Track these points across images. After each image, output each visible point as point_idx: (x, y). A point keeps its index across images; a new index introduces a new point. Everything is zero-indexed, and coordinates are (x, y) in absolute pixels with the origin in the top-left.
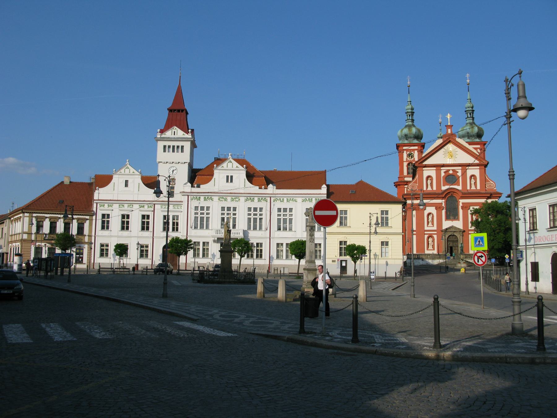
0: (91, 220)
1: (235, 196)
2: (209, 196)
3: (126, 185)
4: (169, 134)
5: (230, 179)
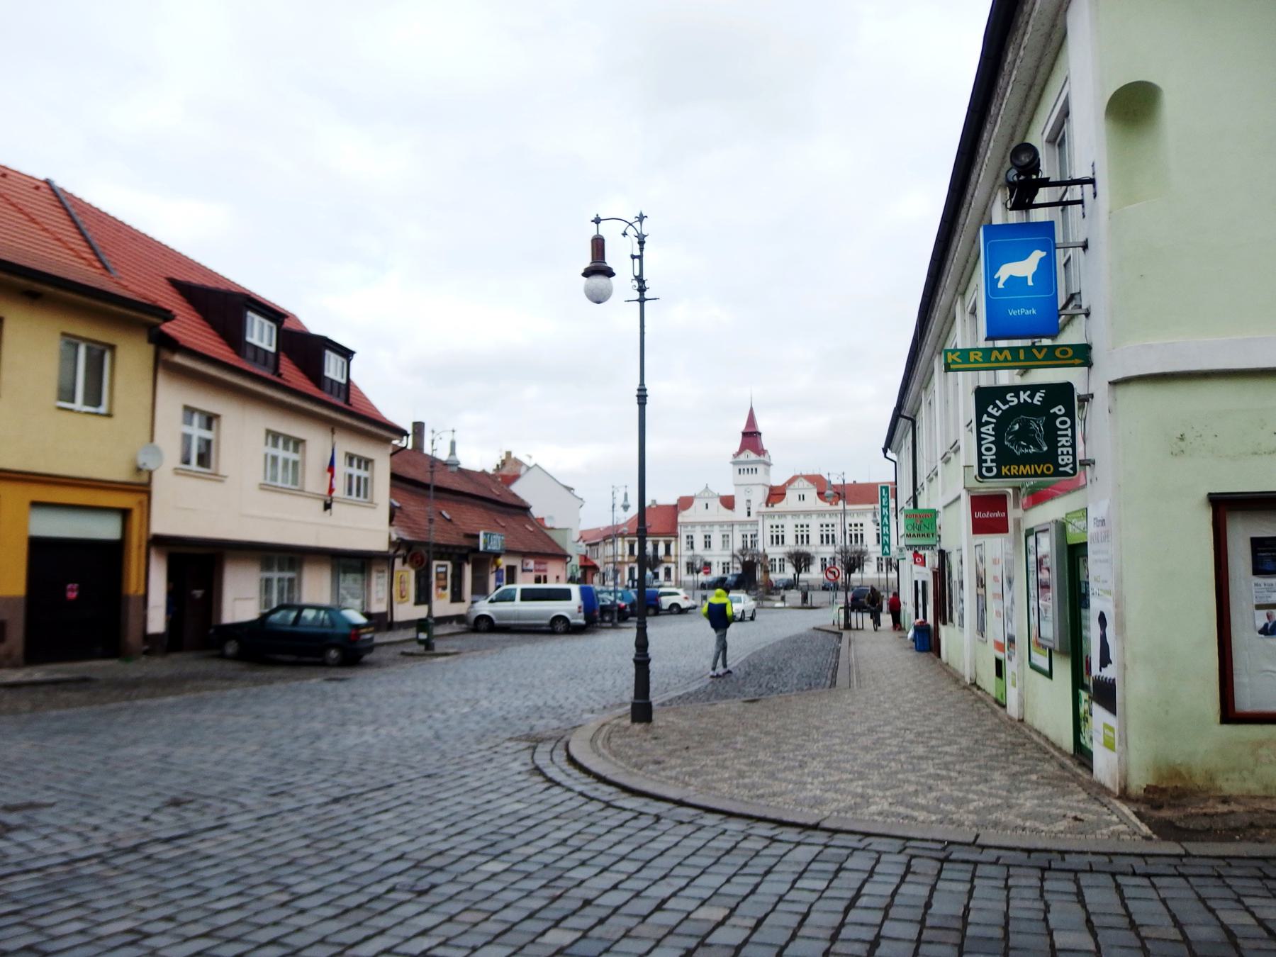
0: (676, 541)
1: (808, 513)
2: (782, 515)
3: (707, 507)
4: (742, 457)
5: (801, 498)
